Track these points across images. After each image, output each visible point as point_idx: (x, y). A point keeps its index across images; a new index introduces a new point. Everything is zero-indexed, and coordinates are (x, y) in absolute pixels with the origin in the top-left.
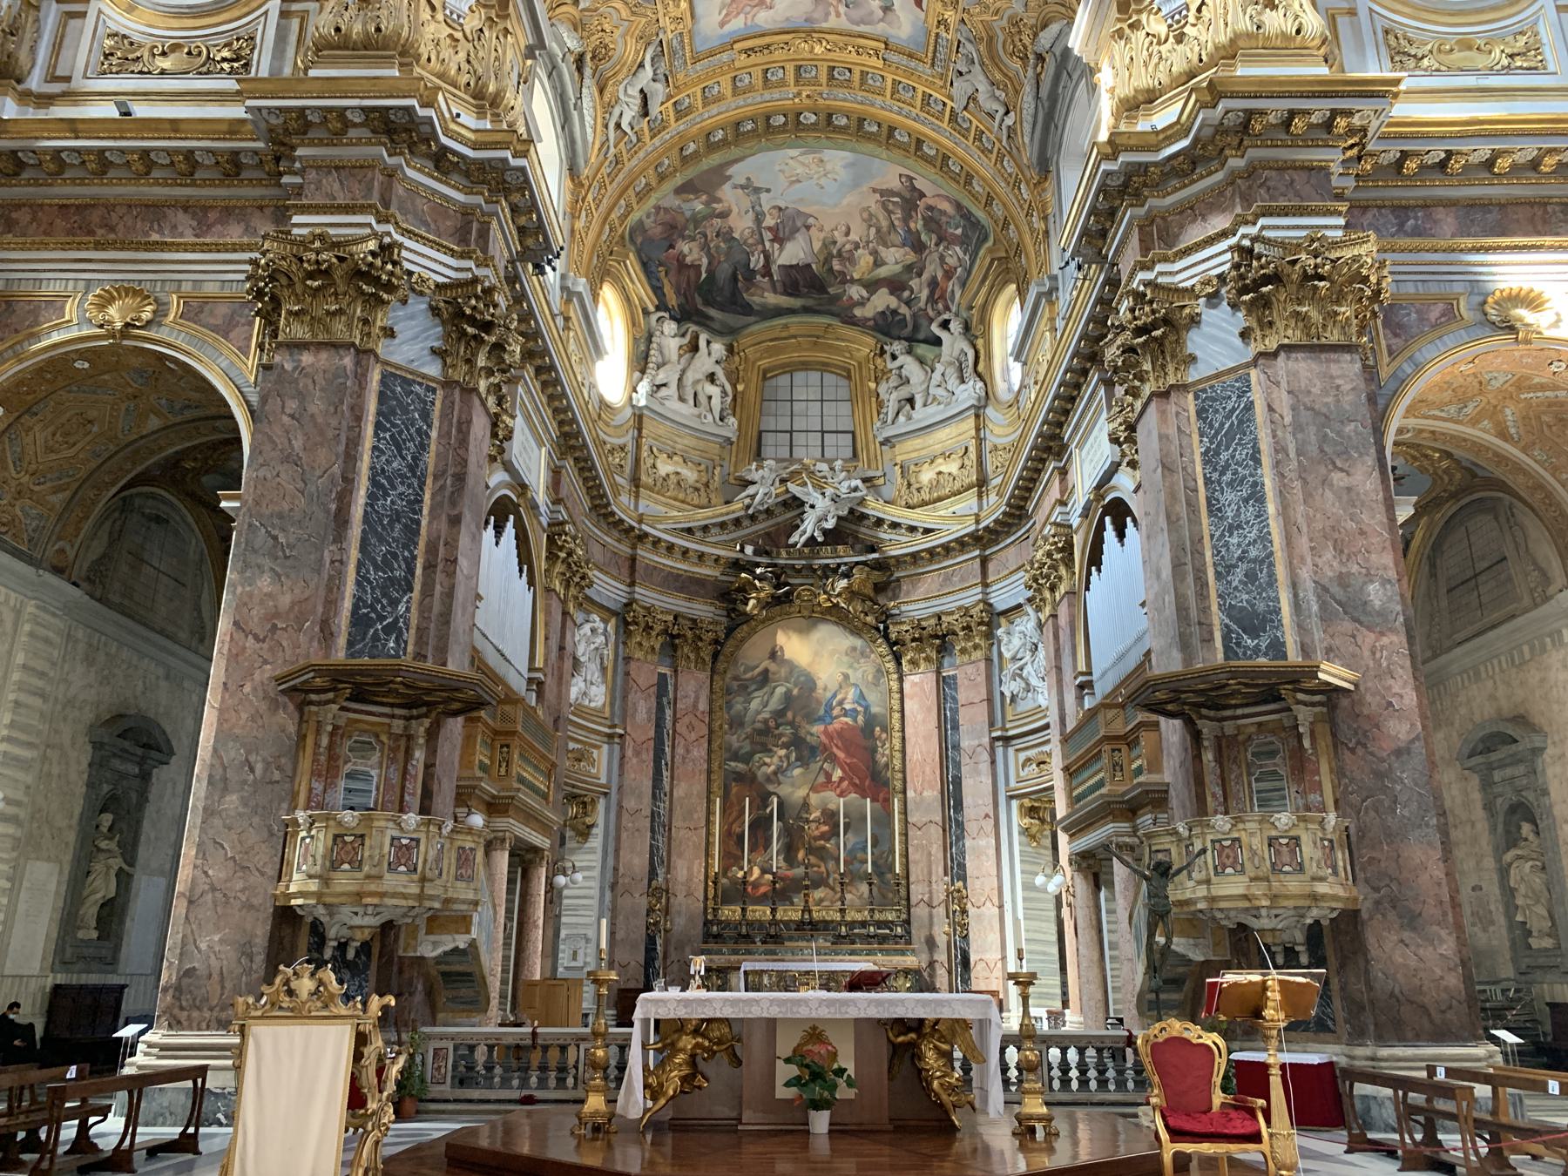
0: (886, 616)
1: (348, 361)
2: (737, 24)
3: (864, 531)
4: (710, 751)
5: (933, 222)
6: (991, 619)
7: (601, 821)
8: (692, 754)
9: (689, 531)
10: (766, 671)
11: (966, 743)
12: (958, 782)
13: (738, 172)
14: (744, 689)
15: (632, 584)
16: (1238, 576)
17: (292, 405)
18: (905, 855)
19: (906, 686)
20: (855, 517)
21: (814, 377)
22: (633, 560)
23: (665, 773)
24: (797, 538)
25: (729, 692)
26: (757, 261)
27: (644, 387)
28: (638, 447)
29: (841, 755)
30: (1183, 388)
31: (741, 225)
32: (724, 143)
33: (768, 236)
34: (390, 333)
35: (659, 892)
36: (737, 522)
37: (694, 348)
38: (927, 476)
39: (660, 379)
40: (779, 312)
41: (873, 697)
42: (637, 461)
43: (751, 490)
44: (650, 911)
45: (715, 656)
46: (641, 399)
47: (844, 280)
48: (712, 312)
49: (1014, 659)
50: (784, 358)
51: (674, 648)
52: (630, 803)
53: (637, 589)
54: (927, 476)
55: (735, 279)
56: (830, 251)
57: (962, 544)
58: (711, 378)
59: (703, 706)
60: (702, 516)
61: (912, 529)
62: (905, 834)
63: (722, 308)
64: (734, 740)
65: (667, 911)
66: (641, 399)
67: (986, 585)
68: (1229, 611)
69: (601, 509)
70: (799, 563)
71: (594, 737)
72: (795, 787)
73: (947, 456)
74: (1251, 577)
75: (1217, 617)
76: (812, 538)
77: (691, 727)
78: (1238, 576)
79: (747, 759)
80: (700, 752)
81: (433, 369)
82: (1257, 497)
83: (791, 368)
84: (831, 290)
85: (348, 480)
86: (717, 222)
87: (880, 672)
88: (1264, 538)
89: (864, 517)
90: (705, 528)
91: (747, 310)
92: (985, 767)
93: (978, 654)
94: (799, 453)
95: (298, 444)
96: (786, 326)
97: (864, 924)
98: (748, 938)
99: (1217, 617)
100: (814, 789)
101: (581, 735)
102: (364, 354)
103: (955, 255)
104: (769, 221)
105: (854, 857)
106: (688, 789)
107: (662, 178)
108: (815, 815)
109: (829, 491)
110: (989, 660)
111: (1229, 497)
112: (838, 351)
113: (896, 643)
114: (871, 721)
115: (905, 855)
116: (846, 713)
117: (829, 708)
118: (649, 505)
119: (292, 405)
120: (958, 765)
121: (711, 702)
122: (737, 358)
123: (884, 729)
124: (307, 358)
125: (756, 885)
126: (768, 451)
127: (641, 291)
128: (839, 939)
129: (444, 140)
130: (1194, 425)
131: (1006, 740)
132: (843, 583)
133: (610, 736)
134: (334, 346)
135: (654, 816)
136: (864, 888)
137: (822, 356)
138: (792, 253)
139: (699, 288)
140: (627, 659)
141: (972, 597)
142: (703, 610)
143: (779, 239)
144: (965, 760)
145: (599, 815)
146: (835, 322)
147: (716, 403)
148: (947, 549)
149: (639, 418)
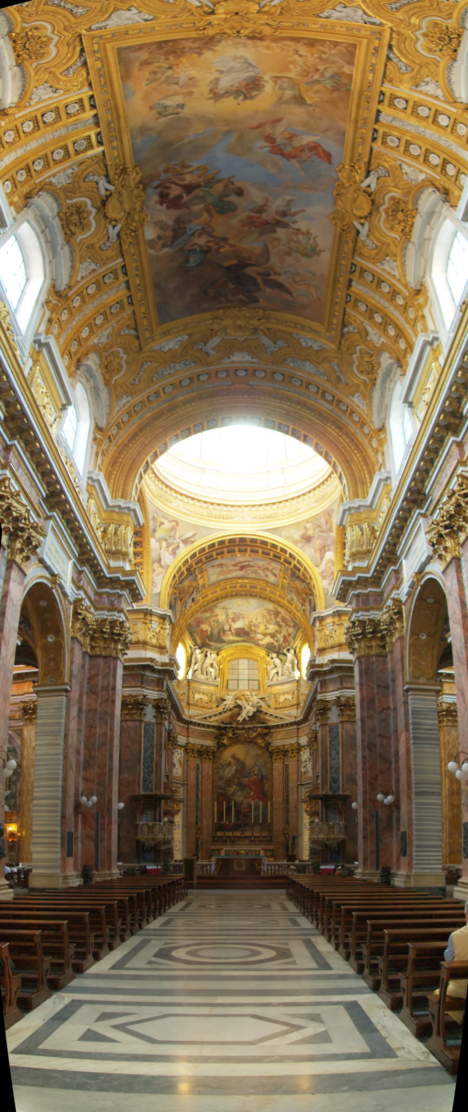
1: (138, 724)
2: (222, 577)
3: (262, 716)
4: (213, 786)
6: (299, 748)
7: (182, 808)
9: (205, 718)
10: (230, 762)
11: (291, 785)
12: (288, 796)
13: (221, 605)
14: (223, 767)
15: (188, 737)
16: (333, 770)
17: (127, 735)
18: (271, 817)
19: (274, 767)
20: (259, 711)
21: (246, 661)
22: (188, 728)
23: (200, 794)
24: (240, 719)
25: (218, 768)
26: (227, 627)
27: (190, 673)
28: (189, 692)
29: (253, 788)
30: (326, 724)
31: (222, 618)
32: (217, 599)
33: (230, 620)
34: (145, 714)
36: (220, 713)
37: (206, 656)
39: (196, 667)
40: (234, 642)
41: (263, 770)
42: (188, 697)
43: (225, 703)
44: (197, 834)
45: (214, 757)
46: (190, 677)
47: (255, 632)
48: (212, 643)
49: (305, 761)
50: (235, 656)
51: (201, 755)
52: (190, 804)
53: (190, 738)
54: (282, 699)
55: (219, 633)
57: (291, 724)
58: (212, 665)
59: (210, 773)
61: (277, 717)
62: (272, 811)
63: (215, 642)
64: (221, 783)
65: (201, 833)
66: (190, 677)
67: (298, 737)
68: (331, 777)
69: (180, 718)
70: (240, 726)
71: (179, 786)
73: (288, 693)
74: (335, 771)
75: (329, 779)
76: (245, 719)
77: (207, 780)
78: (333, 770)
79: (224, 789)
80: (210, 787)
81: (154, 721)
82: (338, 753)
83: (238, 659)
84: (252, 635)
85: (140, 751)
86: (214, 618)
87: (265, 762)
88: (338, 763)
89: (261, 711)
90: (210, 717)
91: (223, 642)
92: (295, 793)
93: (295, 759)
94: (241, 687)
95: (129, 744)
96: (236, 646)
97: (259, 837)
98: (225, 841)
99: (329, 779)
100: (245, 798)
101: (175, 785)
102: (141, 721)
104: (231, 616)
105: (257, 818)
107: (197, 612)
108: (245, 806)
109: (251, 703)
110: (298, 761)
111: (333, 752)
112: (254, 654)
113: (272, 753)
114: (263, 777)
115: (271, 817)
116: (255, 775)
117: (250, 773)
119: (127, 735)
120: (288, 791)
121: (213, 771)
122: (220, 657)
123: (267, 780)
124: (129, 723)
125: (227, 826)
126: (230, 687)
128: (252, 841)
129: (156, 667)
130: (328, 734)
131: (302, 785)
132: (255, 734)
133: (183, 784)
134: (135, 720)
135: (197, 807)
136: (259, 827)
137: (249, 656)
138: (239, 625)
139: (208, 637)
140: (187, 761)
141: (294, 741)
142: (209, 743)
143: (234, 620)
144: (290, 790)
146: (252, 645)
147: (213, 674)
148: (287, 725)
149: (189, 681)
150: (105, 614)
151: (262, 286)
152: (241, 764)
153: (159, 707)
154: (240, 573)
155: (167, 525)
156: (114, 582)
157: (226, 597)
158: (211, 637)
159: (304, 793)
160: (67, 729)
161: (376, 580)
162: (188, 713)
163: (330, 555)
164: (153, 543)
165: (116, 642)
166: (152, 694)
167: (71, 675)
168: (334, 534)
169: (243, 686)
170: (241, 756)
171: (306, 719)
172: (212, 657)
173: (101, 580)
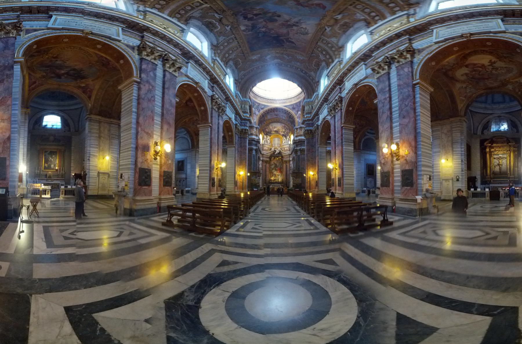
0: (282, 160)
5: (287, 128)
6: (290, 161)
8: (268, 170)
13: (271, 124)
14: (271, 165)
31: (271, 128)
35: (266, 180)
38: (286, 149)
54: (286, 149)
56: (278, 129)
60: (268, 152)
69: (261, 153)
72: (275, 173)
103: (288, 131)
106: (268, 173)
118: (264, 152)
127: (263, 134)
138: (275, 129)
141: (288, 159)
142: (268, 159)
145: (261, 175)
149: (263, 144)
150: (243, 127)
151: (285, 42)
152: (276, 165)
153: (256, 150)
154: (276, 117)
155: (257, 105)
156: (245, 120)
157: (272, 122)
158: (268, 132)
159: (291, 172)
160: (235, 156)
161: (312, 120)
162: (263, 152)
163: (299, 112)
164: (253, 109)
165: (246, 134)
166: (255, 147)
167: (236, 143)
168: (301, 107)
169: (276, 145)
170: (276, 163)
171: (292, 154)
172: (269, 137)
173: (241, 119)
